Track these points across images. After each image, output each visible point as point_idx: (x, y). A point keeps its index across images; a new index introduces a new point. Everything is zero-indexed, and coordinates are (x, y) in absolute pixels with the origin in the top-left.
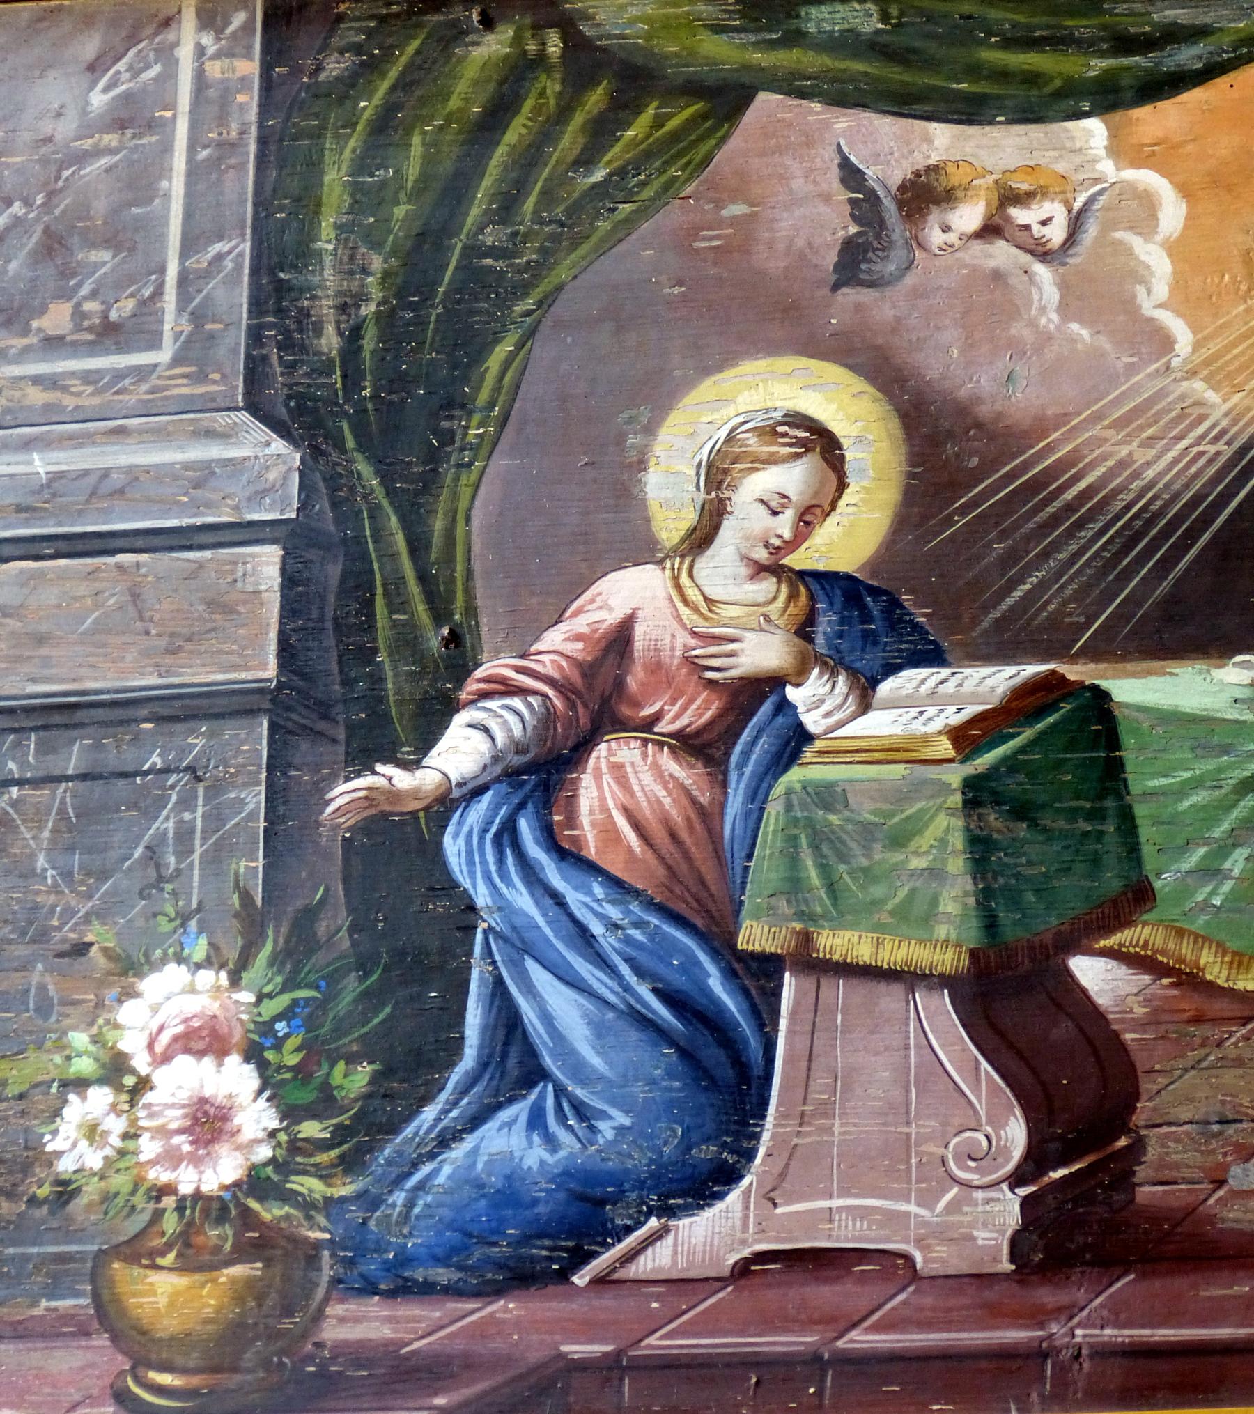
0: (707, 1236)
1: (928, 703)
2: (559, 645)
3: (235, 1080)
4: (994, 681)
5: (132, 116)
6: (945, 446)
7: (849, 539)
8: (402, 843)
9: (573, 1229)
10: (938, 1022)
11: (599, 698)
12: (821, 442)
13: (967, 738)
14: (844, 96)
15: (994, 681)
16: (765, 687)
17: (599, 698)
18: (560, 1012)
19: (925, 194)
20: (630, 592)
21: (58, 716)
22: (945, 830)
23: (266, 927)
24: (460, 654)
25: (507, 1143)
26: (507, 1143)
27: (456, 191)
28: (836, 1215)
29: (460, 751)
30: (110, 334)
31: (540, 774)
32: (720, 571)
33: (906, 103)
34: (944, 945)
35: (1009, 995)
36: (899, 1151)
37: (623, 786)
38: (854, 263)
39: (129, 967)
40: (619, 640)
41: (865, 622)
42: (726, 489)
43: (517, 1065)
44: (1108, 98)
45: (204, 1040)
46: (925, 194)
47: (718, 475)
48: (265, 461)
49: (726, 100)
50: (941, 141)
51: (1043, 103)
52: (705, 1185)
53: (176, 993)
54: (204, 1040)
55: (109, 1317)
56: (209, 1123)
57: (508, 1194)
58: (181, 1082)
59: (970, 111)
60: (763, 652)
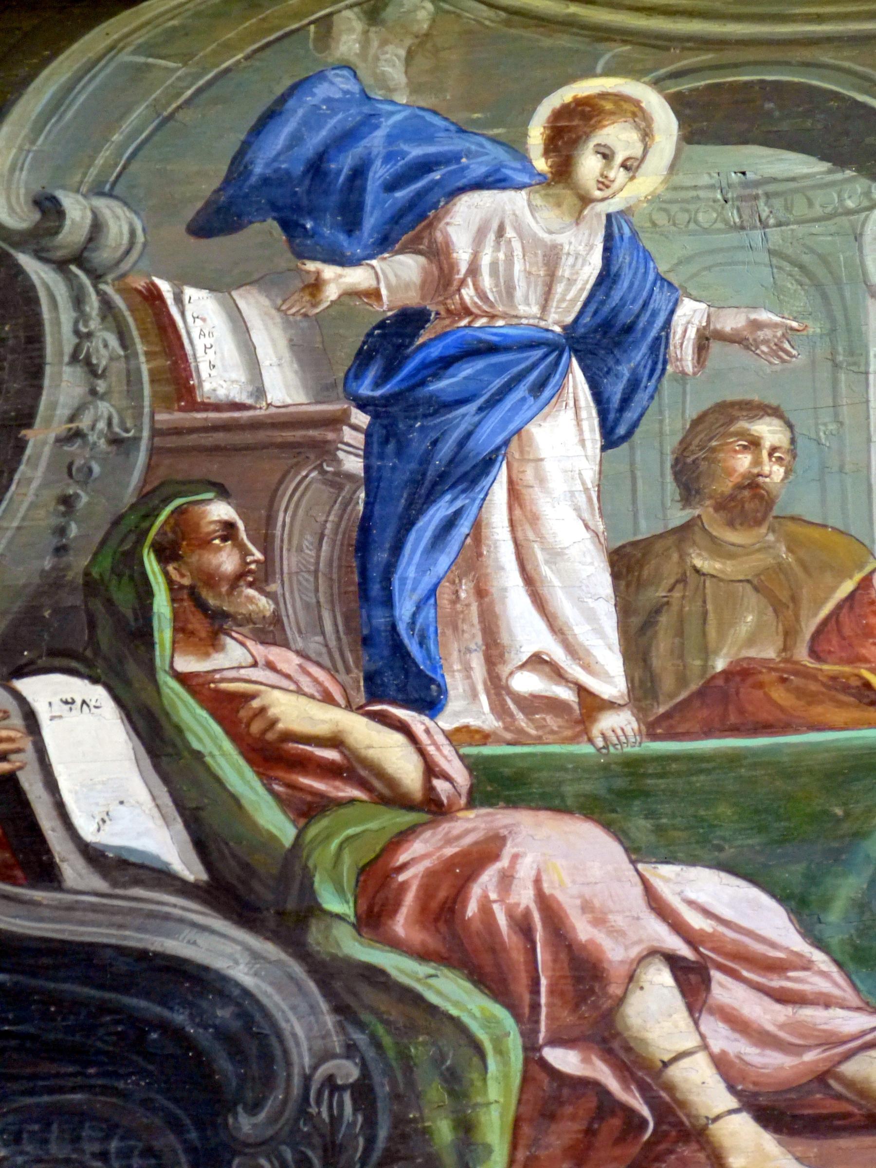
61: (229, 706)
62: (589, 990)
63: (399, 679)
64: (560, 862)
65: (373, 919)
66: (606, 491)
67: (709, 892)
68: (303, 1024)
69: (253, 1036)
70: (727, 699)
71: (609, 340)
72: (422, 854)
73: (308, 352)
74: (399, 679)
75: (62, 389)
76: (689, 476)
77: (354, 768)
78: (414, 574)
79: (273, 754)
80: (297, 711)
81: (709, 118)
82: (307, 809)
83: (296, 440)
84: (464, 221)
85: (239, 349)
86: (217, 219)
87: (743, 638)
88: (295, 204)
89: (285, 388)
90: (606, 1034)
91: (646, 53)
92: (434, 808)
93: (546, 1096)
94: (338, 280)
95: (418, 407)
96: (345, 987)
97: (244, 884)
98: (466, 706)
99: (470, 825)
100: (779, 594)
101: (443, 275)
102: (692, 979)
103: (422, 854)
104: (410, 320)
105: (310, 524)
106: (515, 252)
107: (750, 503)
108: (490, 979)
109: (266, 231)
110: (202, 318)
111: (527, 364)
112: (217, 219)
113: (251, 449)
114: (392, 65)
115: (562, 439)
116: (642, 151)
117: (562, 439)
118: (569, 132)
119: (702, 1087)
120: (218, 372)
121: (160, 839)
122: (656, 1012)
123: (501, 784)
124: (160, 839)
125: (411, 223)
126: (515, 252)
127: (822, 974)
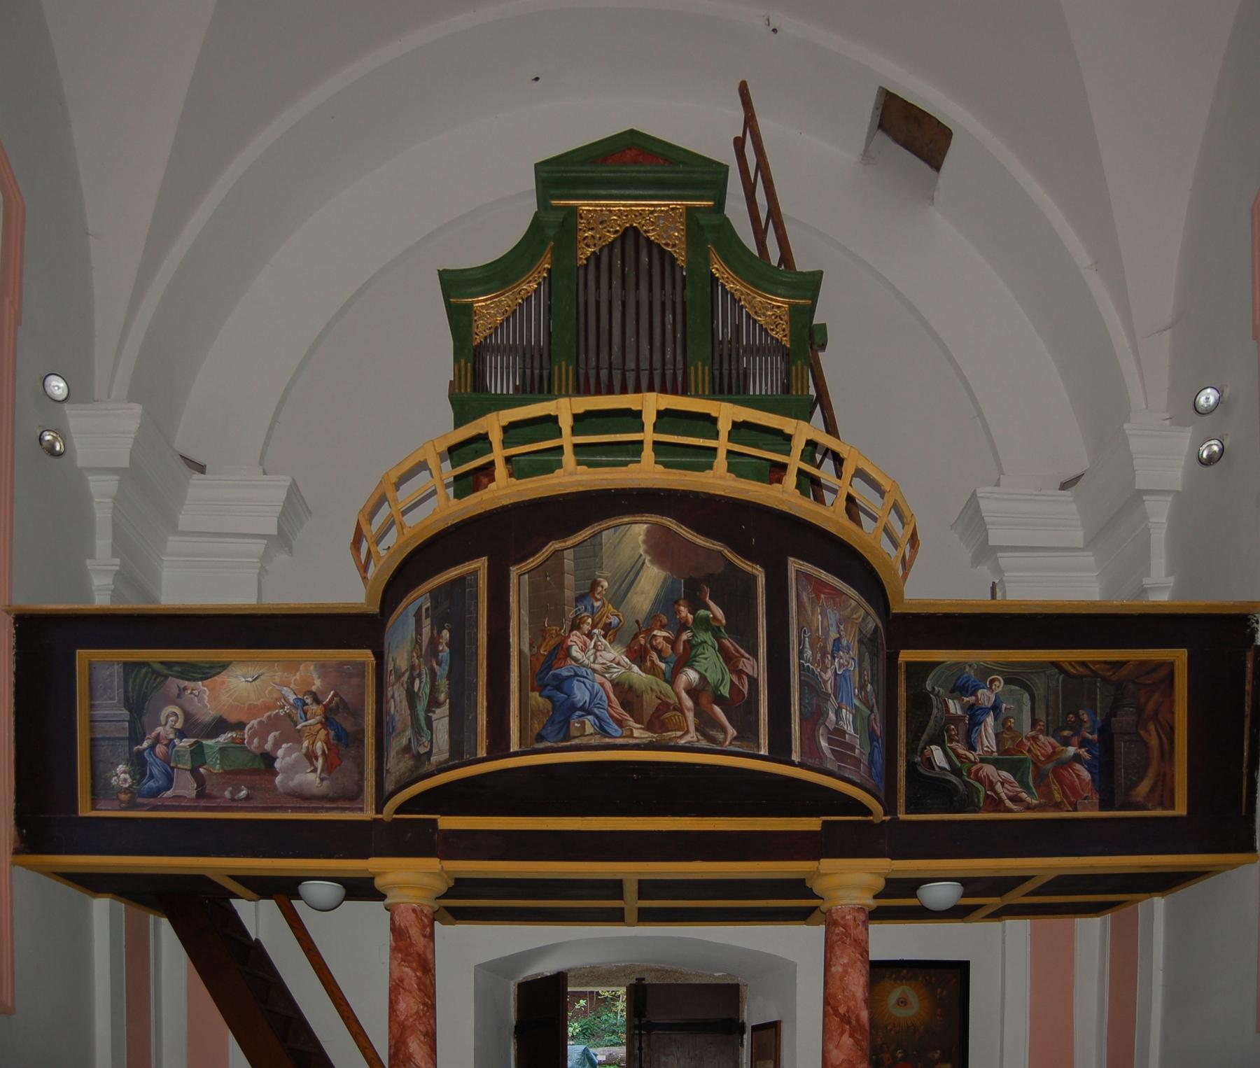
0: (169, 793)
1: (187, 742)
2: (154, 734)
3: (127, 776)
4: (193, 740)
5: (111, 675)
6: (188, 716)
7: (179, 725)
8: (141, 753)
9: (156, 793)
10: (188, 773)
11: (157, 740)
12: (176, 715)
13: (191, 746)
14: (178, 677)
15: (193, 740)
16: (171, 740)
17: (157, 740)
18: (156, 771)
19: (185, 689)
20: (159, 729)
21: (109, 739)
22: (188, 756)
23: (129, 762)
24: (145, 735)
25: (151, 784)
26: (151, 784)
27: (142, 685)
28: (180, 792)
29: (145, 745)
30: (111, 699)
31: (152, 747)
32: (168, 727)
33: (183, 679)
34: (188, 767)
35: (194, 772)
36: (185, 787)
37: (160, 749)
38: (179, 696)
39: (117, 765)
40: (159, 734)
41: (181, 734)
42: (169, 719)
43: (152, 776)
44: (202, 679)
45: (124, 772)
46: (185, 689)
47: (167, 717)
48: (125, 713)
49: (166, 677)
50: (186, 683)
51: (196, 680)
52: (168, 788)
53: (121, 768)
54: (124, 772)
55: (118, 799)
56: (125, 780)
57: (152, 788)
58: (122, 776)
59: (189, 680)
60: (172, 736)
61: (954, 750)
62: (992, 786)
63: (972, 748)
64: (989, 770)
65: (969, 776)
66: (995, 726)
67: (1005, 774)
68: (961, 787)
69: (956, 788)
70: (1007, 752)
71: (995, 708)
72: (974, 768)
73: (962, 708)
74: (972, 748)
75: (935, 711)
76: (1004, 725)
77: (967, 758)
78: (973, 736)
79: (958, 756)
80: (961, 751)
81: (1007, 681)
82: (962, 762)
83: (960, 719)
84: (980, 692)
85: (954, 707)
86: (952, 691)
87: (1008, 745)
88: (961, 689)
89: (959, 713)
90: (993, 790)
91: (1000, 673)
92: (975, 763)
93: (987, 796)
94: (966, 699)
95: (974, 715)
96: (967, 784)
97: (955, 771)
98: (979, 752)
99: (979, 765)
100: (1013, 739)
101: (977, 699)
102: (1002, 784)
103: (974, 768)
104: (973, 705)
105: (962, 730)
106: (985, 697)
107: (1010, 729)
108: (981, 783)
109: (957, 693)
110: (950, 703)
111: (986, 711)
112: (952, 691)
113: (955, 720)
114: (972, 673)
115: (990, 720)
116: (1000, 685)
117: (990, 720)
118: (992, 681)
119: (1003, 795)
120: (952, 710)
121: (946, 766)
122: (998, 787)
123: (983, 760)
124: (946, 766)
125: (974, 693)
126: (985, 697)
127: (1016, 784)
